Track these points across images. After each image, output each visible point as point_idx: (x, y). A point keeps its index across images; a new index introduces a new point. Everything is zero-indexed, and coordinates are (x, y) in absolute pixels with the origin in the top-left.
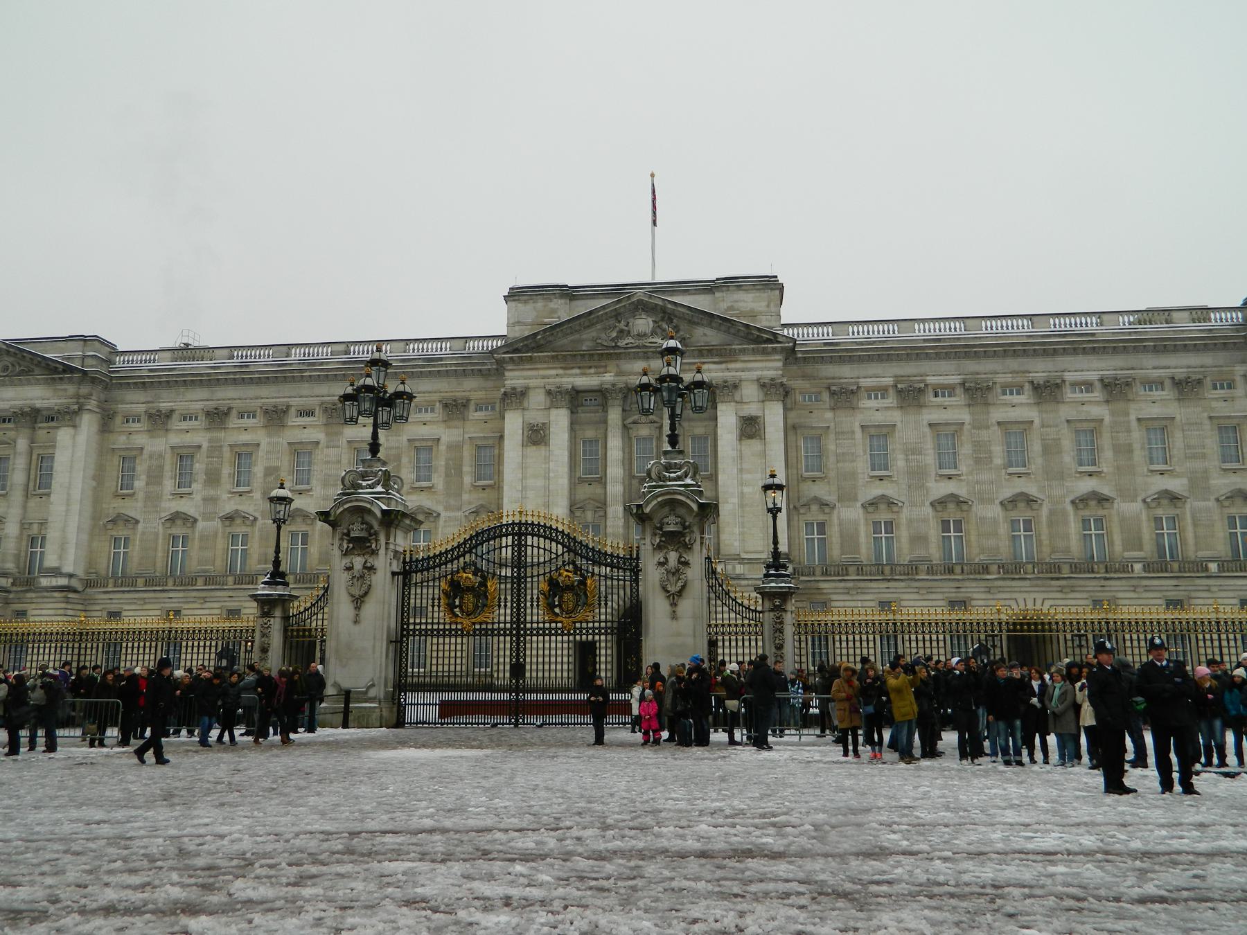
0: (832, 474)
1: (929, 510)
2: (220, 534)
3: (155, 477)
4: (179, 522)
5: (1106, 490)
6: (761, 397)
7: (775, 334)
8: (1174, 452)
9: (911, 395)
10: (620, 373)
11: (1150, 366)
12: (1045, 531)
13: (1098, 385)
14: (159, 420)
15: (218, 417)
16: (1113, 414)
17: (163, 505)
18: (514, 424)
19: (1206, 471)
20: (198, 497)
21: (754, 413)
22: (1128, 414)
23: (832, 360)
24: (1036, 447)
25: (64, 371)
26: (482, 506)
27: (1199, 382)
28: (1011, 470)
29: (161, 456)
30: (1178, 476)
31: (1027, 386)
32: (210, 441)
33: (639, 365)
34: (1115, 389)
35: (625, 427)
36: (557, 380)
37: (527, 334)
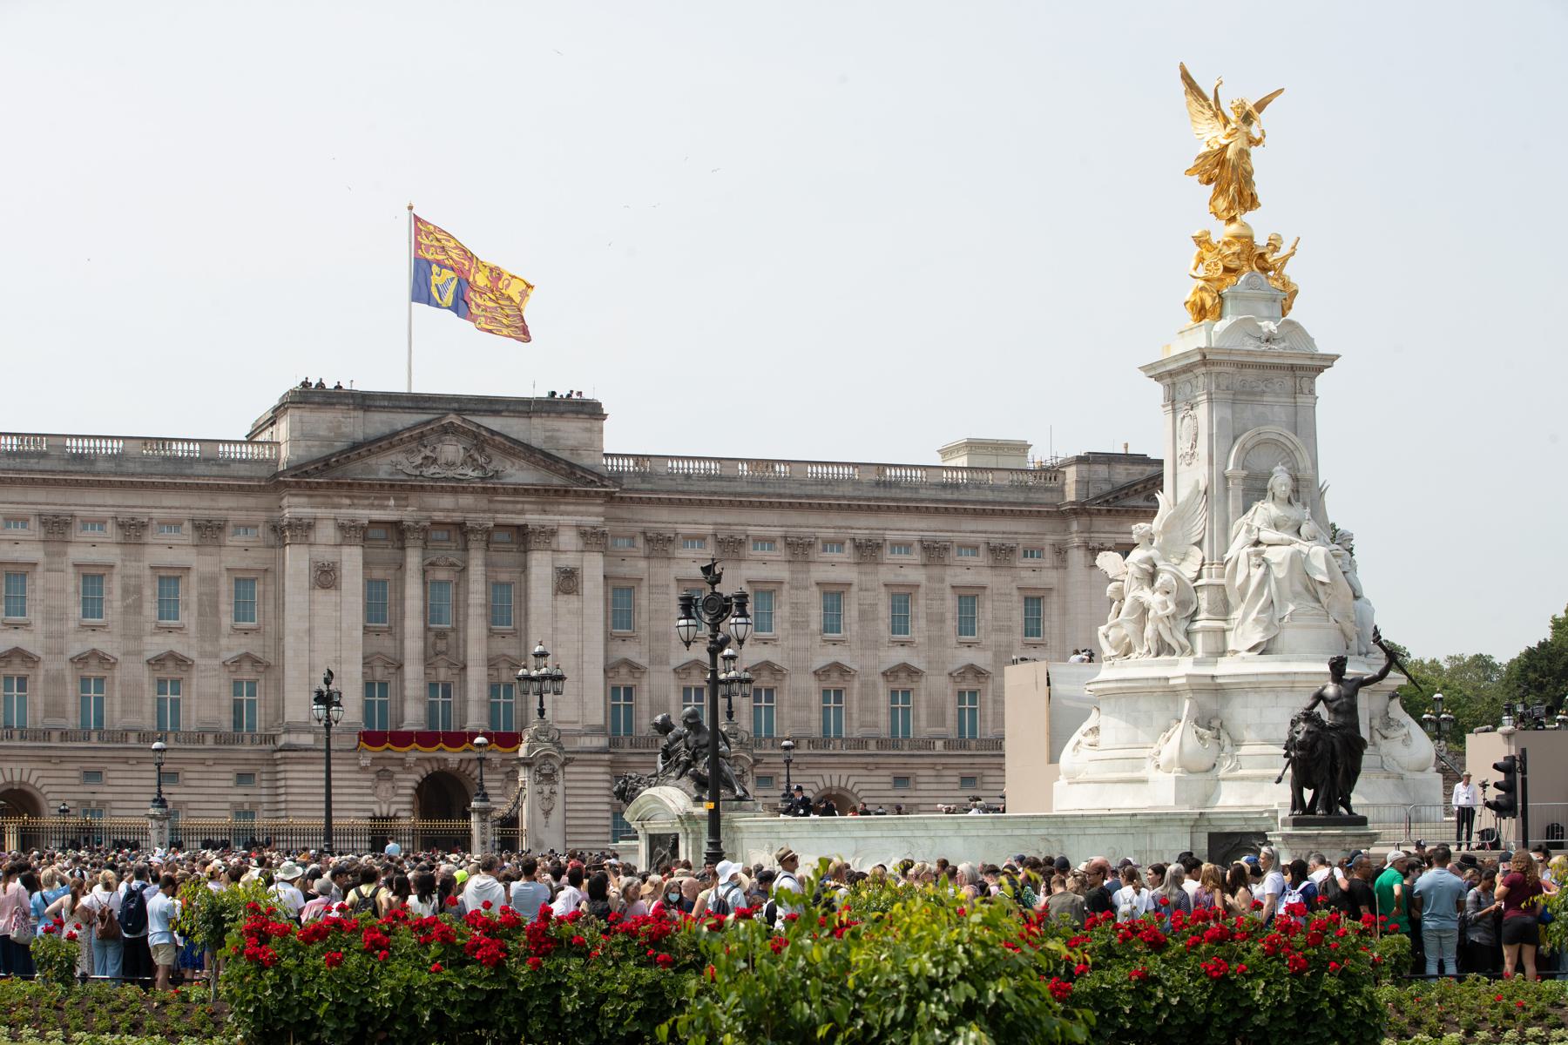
0: (644, 633)
5: (916, 662)
6: (580, 546)
7: (601, 477)
8: (982, 623)
12: (855, 704)
13: (917, 546)
16: (929, 579)
18: (297, 561)
19: (1010, 646)
22: (942, 580)
26: (247, 656)
27: (1012, 550)
30: (984, 649)
31: (848, 544)
33: (447, 501)
34: (934, 552)
35: (425, 572)
36: (351, 511)
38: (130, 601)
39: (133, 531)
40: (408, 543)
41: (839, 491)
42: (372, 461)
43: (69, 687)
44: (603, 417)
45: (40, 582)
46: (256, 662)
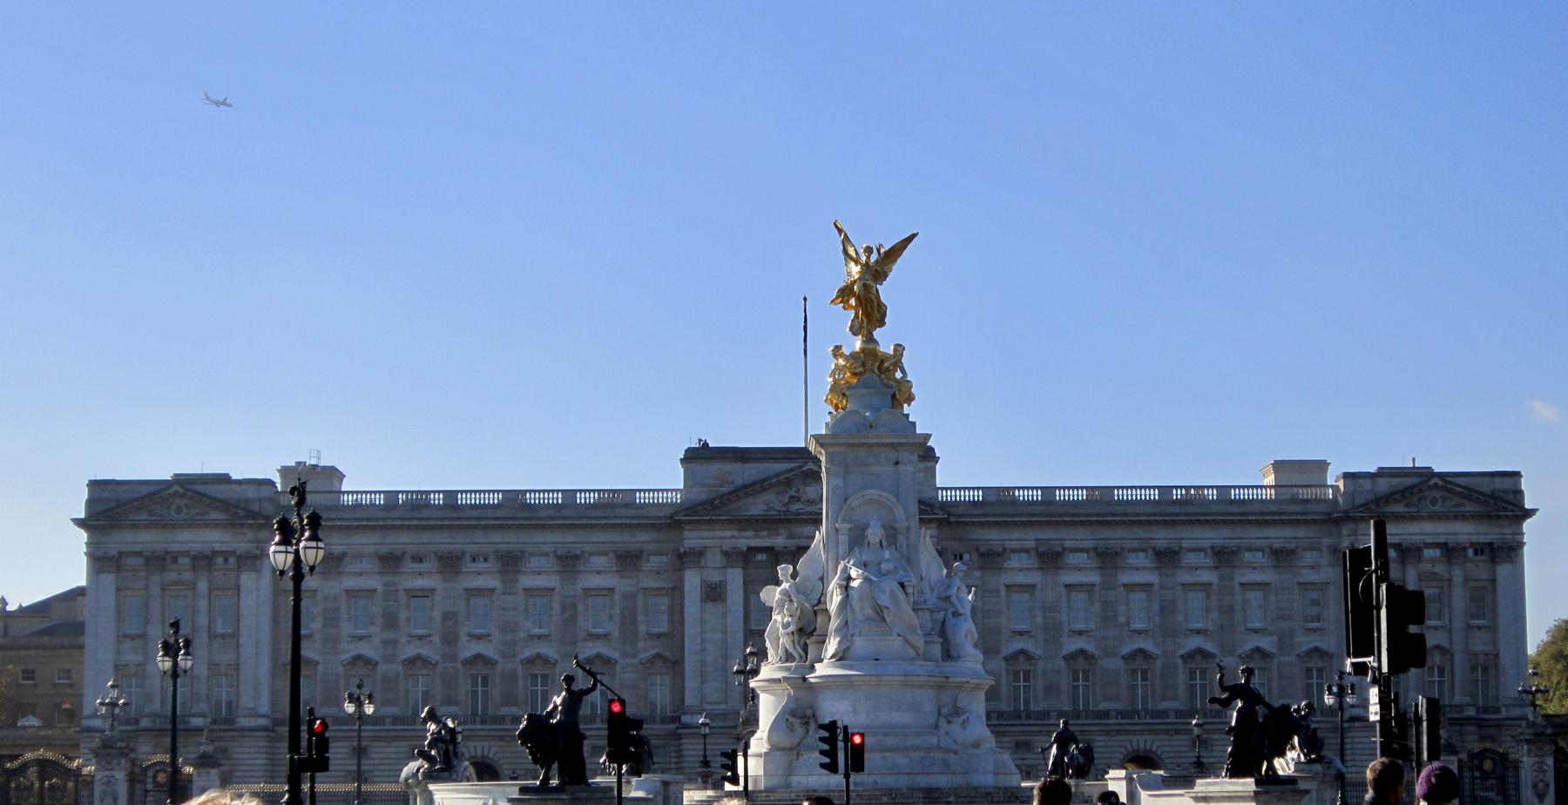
1: (1062, 663)
5: (1209, 647)
9: (1050, 559)
10: (791, 536)
11: (1253, 534)
15: (390, 562)
16: (1221, 578)
18: (692, 581)
20: (376, 640)
22: (1231, 578)
23: (981, 524)
26: (658, 655)
27: (1292, 552)
29: (336, 598)
31: (1150, 552)
32: (385, 585)
34: (1224, 557)
37: (704, 497)
39: (569, 562)
41: (1142, 509)
42: (750, 500)
44: (936, 460)
46: (666, 660)
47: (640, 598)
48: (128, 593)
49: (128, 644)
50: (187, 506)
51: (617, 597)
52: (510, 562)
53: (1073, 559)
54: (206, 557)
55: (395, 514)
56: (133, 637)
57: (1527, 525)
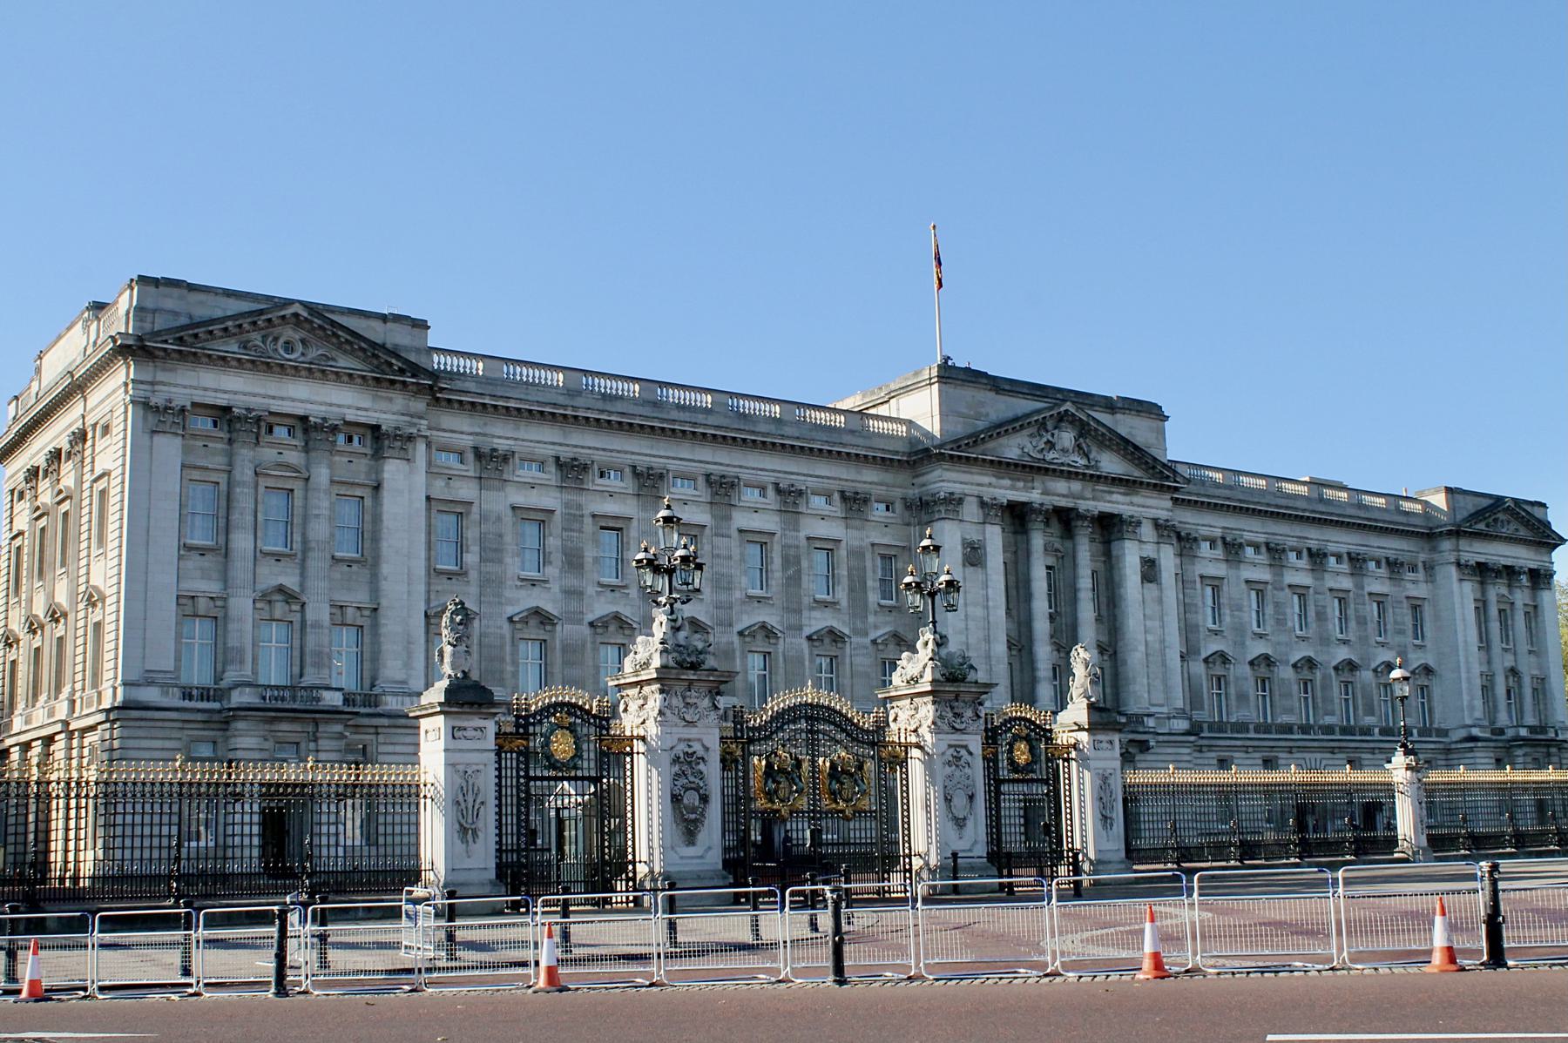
2: (589, 645)
3: (492, 552)
4: (533, 622)
7: (1175, 472)
9: (1233, 549)
10: (1045, 493)
13: (1345, 557)
14: (491, 462)
16: (1356, 586)
17: (508, 593)
18: (950, 535)
20: (555, 588)
21: (1153, 555)
24: (1311, 613)
25: (402, 371)
27: (1402, 564)
28: (1298, 632)
32: (567, 505)
33: (1061, 486)
34: (1356, 562)
38: (790, 572)
39: (790, 497)
40: (1030, 525)
42: (1003, 440)
43: (738, 661)
45: (707, 548)
47: (868, 556)
48: (196, 475)
49: (194, 562)
50: (303, 341)
51: (843, 553)
52: (722, 488)
53: (1250, 551)
54: (334, 429)
55: (579, 402)
56: (202, 551)
57: (1557, 555)
